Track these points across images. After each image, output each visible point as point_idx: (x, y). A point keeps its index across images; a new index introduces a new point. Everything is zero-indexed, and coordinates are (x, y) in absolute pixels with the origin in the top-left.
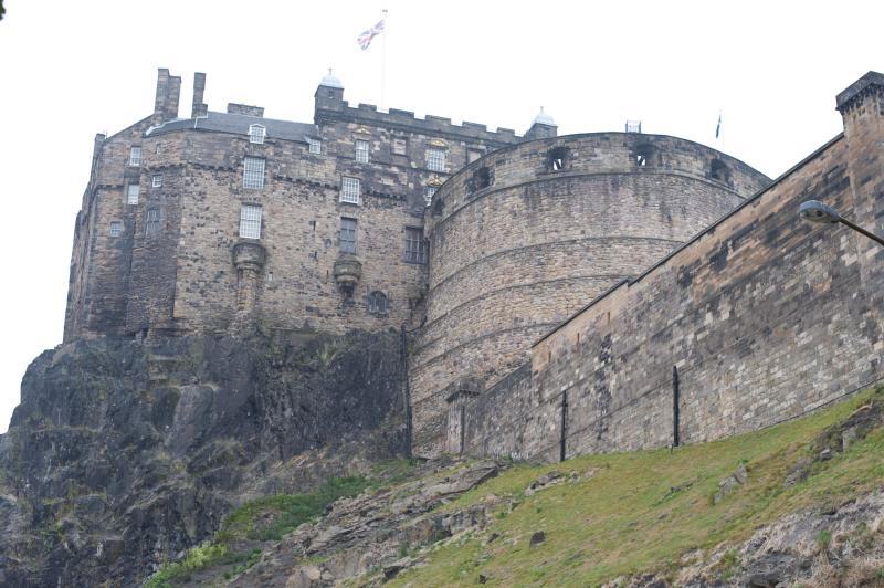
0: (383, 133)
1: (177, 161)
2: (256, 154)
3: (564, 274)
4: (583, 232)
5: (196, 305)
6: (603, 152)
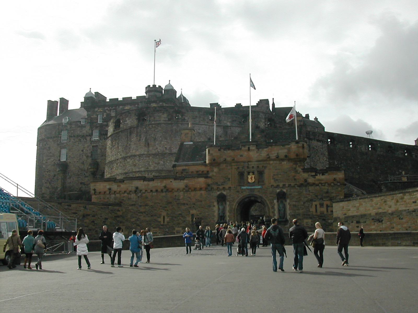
0: (107, 109)
2: (65, 129)
5: (48, 188)
6: (129, 119)
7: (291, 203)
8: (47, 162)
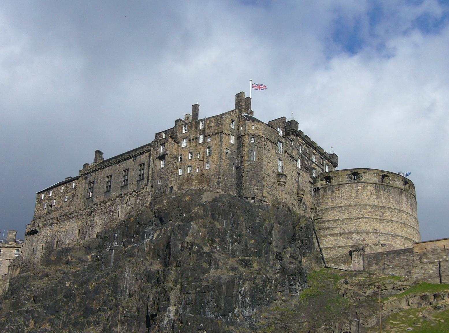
1: (262, 135)
3: (389, 218)
4: (394, 206)
8: (267, 165)
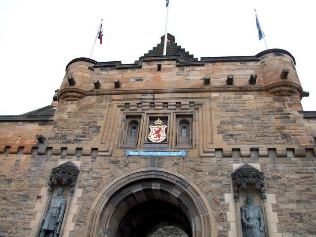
7: (282, 206)
